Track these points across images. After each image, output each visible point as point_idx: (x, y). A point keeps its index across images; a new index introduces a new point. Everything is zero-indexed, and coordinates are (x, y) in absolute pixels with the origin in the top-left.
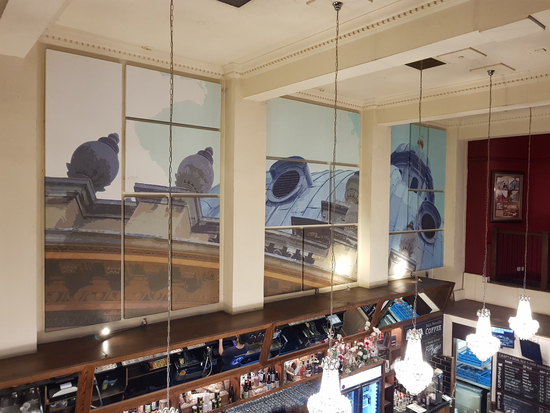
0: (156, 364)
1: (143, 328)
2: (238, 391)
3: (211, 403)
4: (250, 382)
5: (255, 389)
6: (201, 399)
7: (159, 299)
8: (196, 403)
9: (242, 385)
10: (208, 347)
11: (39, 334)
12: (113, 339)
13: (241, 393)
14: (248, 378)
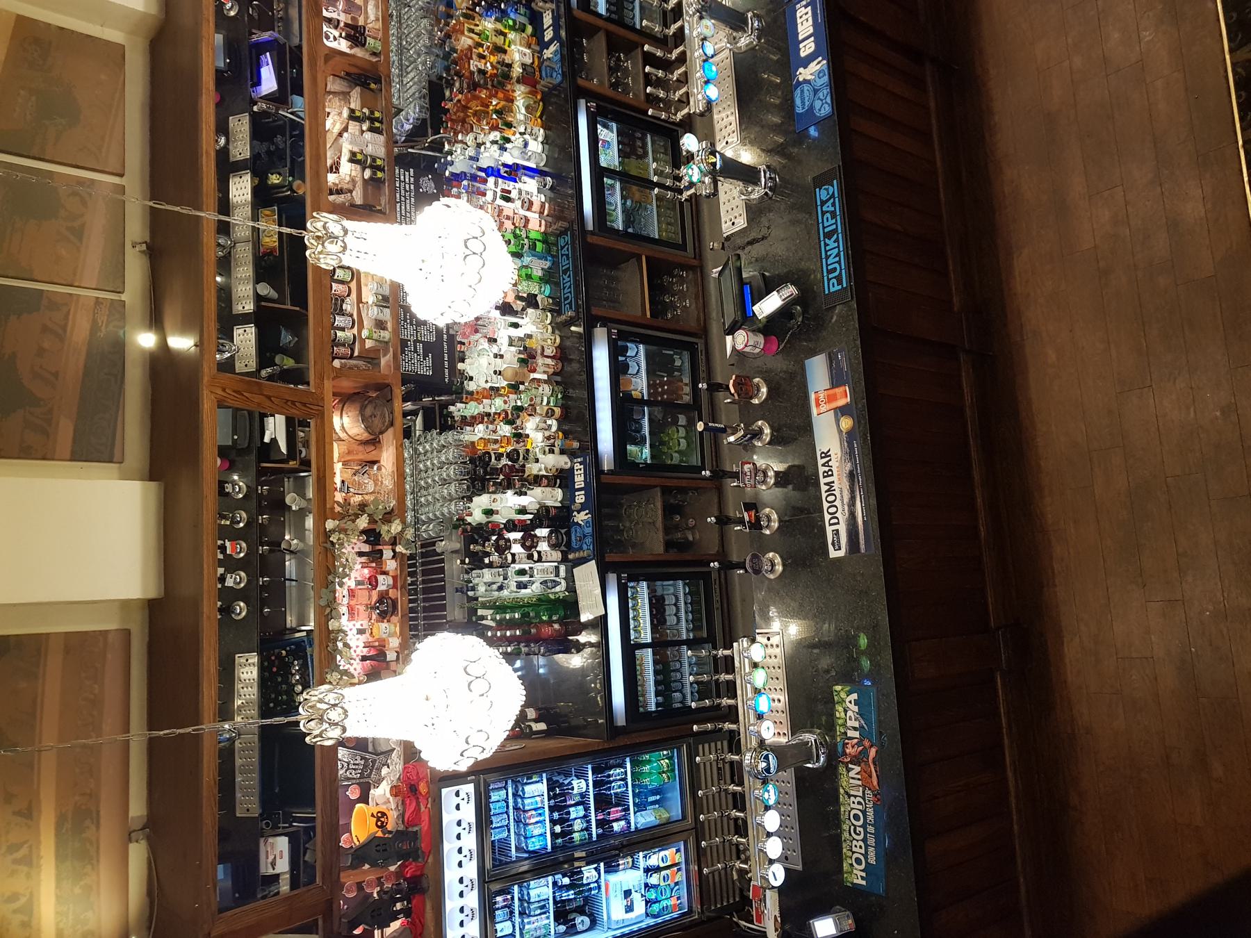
0: (267, 240)
1: (154, 253)
2: (359, 63)
3: (368, 135)
4: (346, 25)
5: (367, 18)
6: (353, 154)
7: (84, 203)
8: (358, 167)
9: (351, 47)
10: (255, 109)
11: (125, 477)
12: (168, 324)
13: (367, 57)
14: (336, 27)
